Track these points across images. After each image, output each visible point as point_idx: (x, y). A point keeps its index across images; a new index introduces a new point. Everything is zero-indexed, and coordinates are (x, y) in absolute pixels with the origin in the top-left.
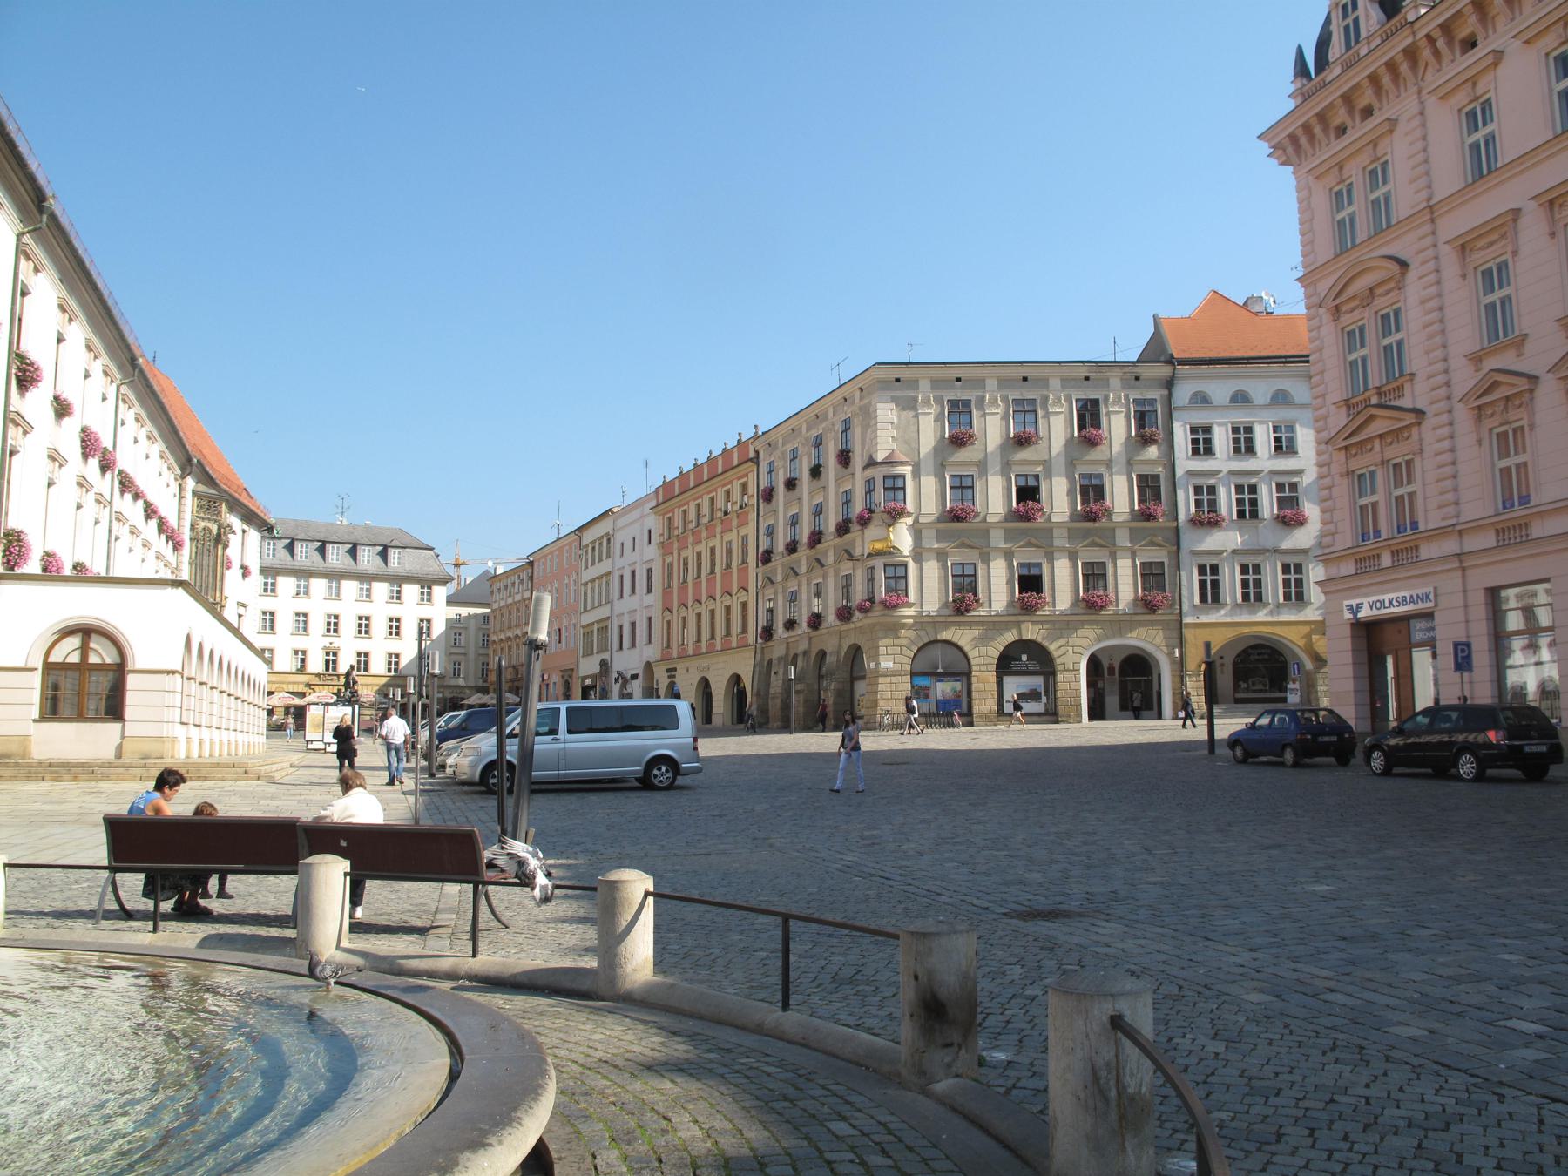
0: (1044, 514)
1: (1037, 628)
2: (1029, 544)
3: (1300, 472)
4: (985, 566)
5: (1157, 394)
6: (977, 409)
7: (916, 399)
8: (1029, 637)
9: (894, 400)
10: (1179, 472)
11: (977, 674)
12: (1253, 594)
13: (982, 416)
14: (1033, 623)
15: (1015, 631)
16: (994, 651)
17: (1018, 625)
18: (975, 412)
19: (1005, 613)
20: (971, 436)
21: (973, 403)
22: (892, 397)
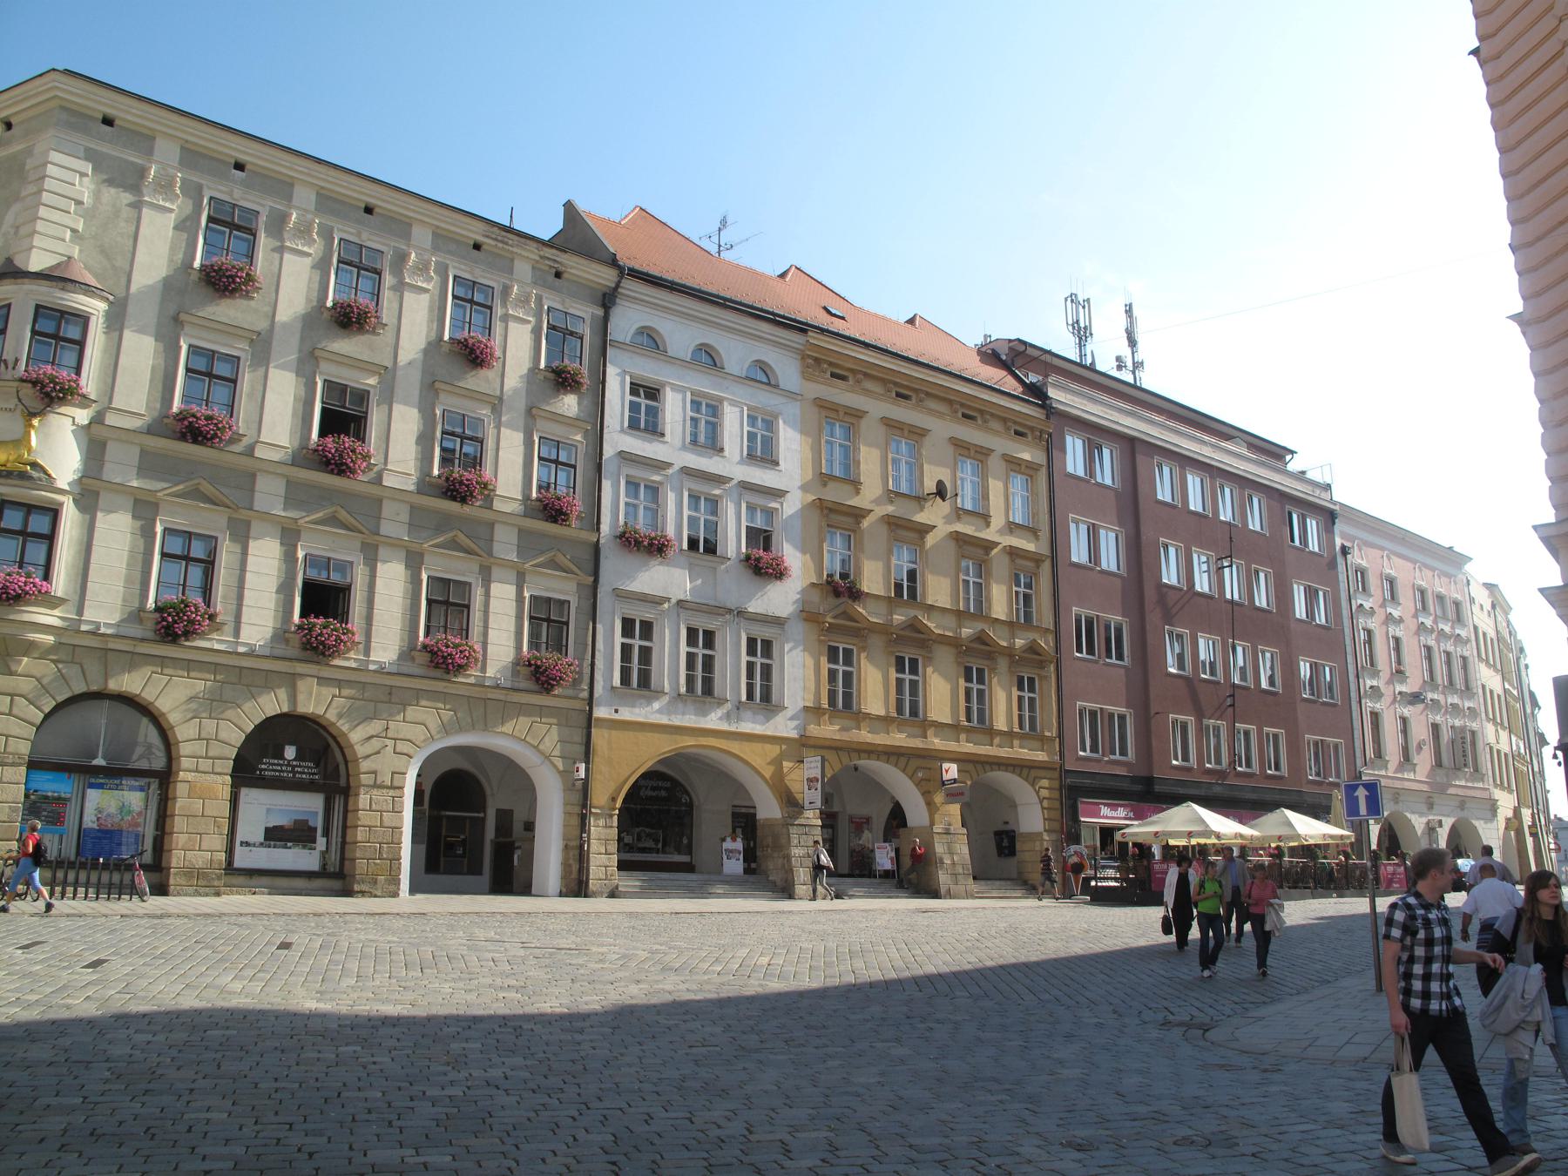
0: (370, 467)
1: (328, 692)
2: (333, 520)
3: (779, 494)
4: (237, 548)
5: (586, 312)
6: (269, 233)
7: (142, 172)
8: (310, 710)
9: (90, 155)
10: (609, 451)
11: (190, 776)
12: (702, 686)
13: (273, 250)
14: (322, 681)
15: (282, 694)
16: (234, 731)
17: (291, 680)
18: (262, 238)
19: (267, 652)
20: (250, 279)
21: (263, 219)
22: (87, 150)
